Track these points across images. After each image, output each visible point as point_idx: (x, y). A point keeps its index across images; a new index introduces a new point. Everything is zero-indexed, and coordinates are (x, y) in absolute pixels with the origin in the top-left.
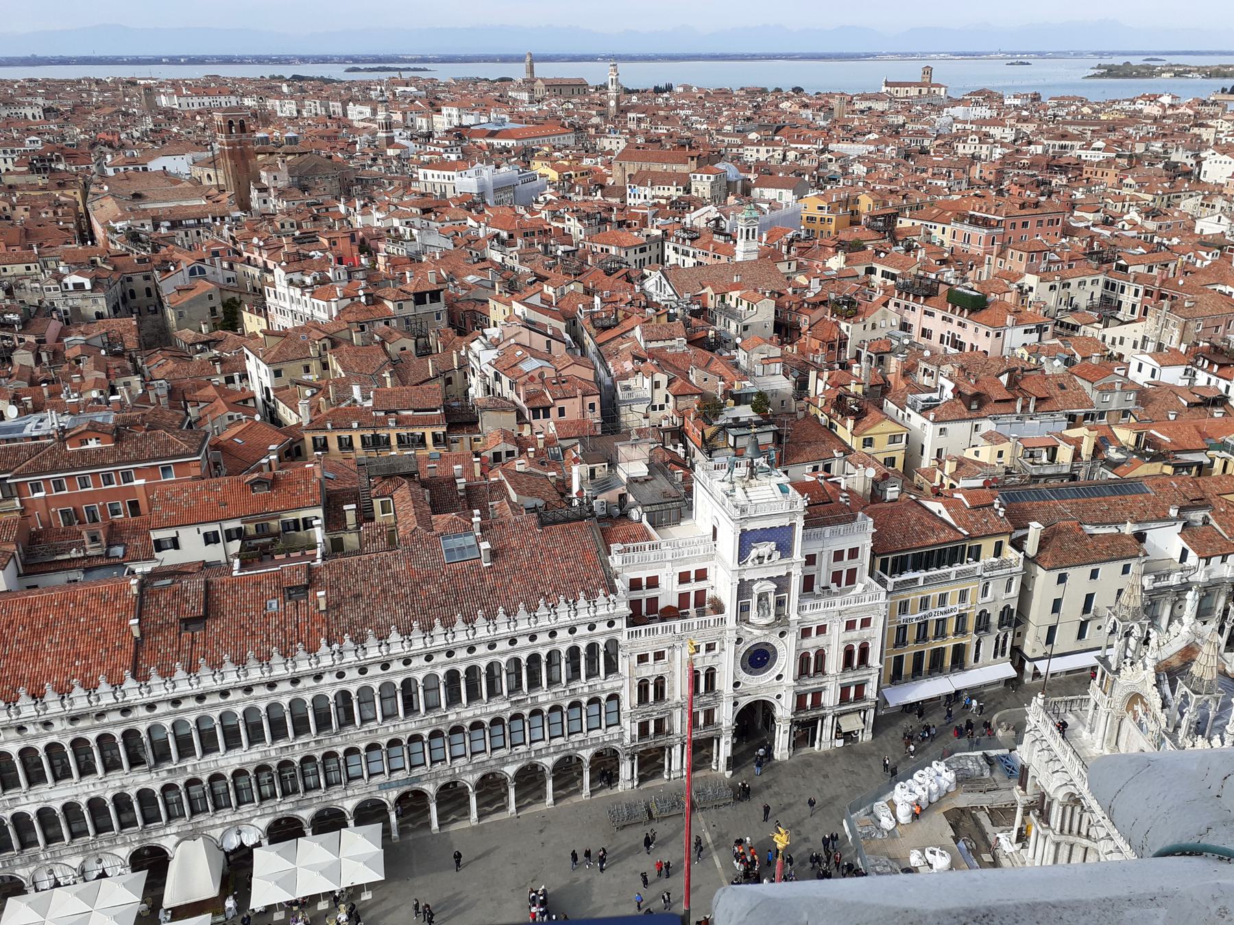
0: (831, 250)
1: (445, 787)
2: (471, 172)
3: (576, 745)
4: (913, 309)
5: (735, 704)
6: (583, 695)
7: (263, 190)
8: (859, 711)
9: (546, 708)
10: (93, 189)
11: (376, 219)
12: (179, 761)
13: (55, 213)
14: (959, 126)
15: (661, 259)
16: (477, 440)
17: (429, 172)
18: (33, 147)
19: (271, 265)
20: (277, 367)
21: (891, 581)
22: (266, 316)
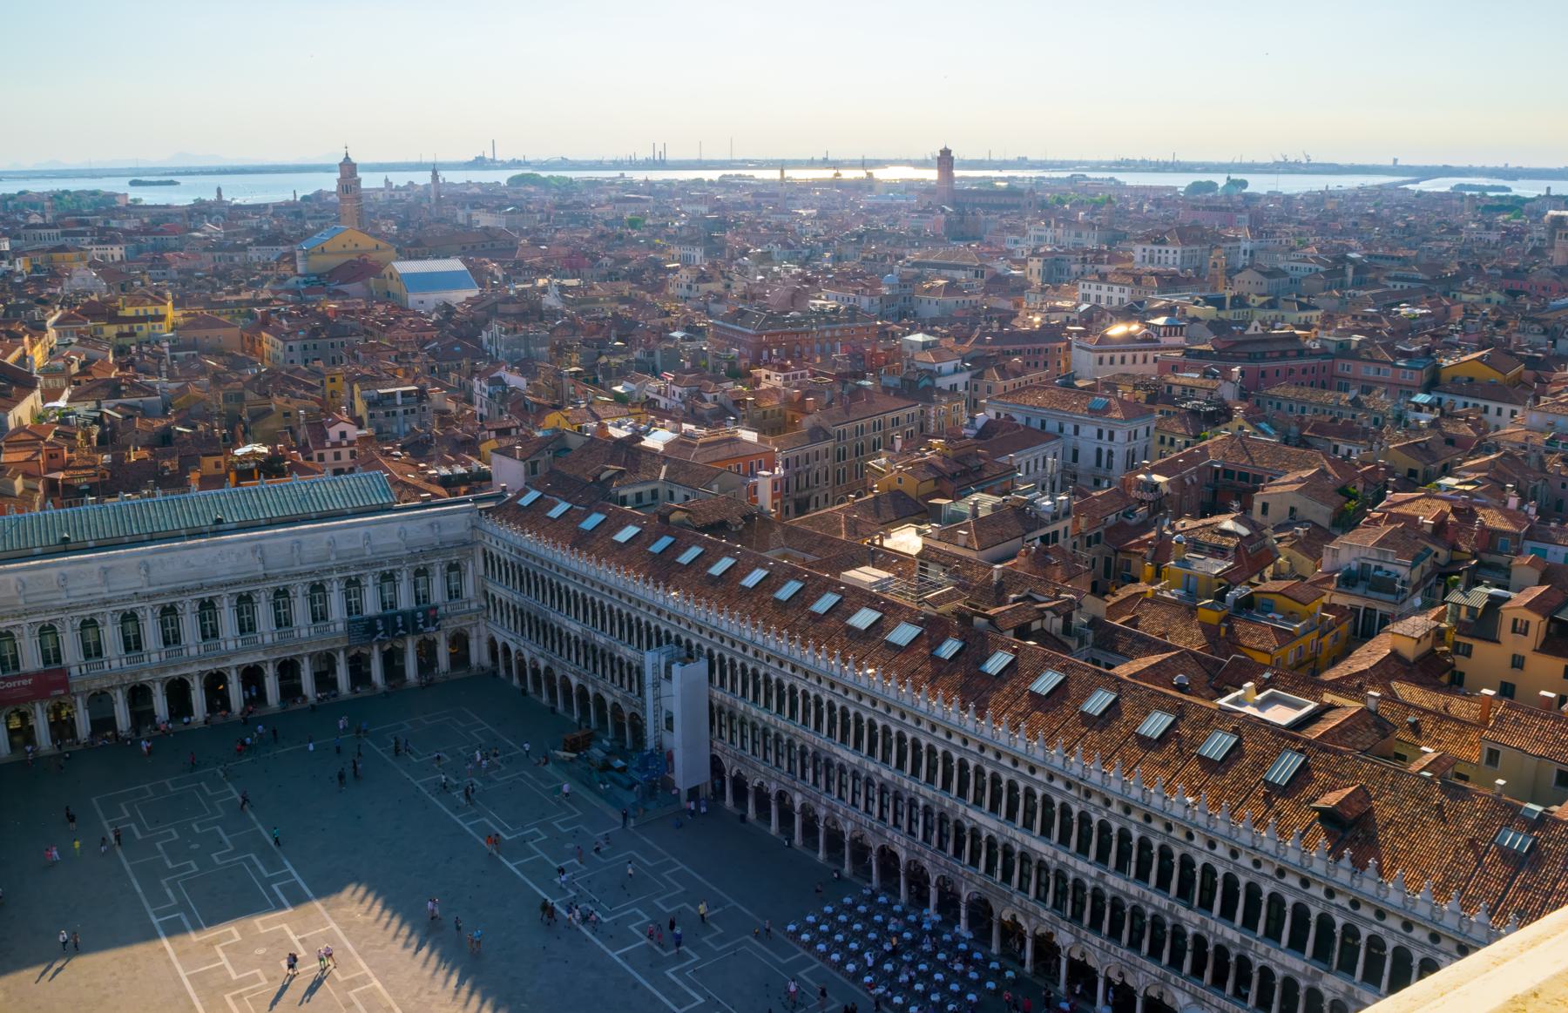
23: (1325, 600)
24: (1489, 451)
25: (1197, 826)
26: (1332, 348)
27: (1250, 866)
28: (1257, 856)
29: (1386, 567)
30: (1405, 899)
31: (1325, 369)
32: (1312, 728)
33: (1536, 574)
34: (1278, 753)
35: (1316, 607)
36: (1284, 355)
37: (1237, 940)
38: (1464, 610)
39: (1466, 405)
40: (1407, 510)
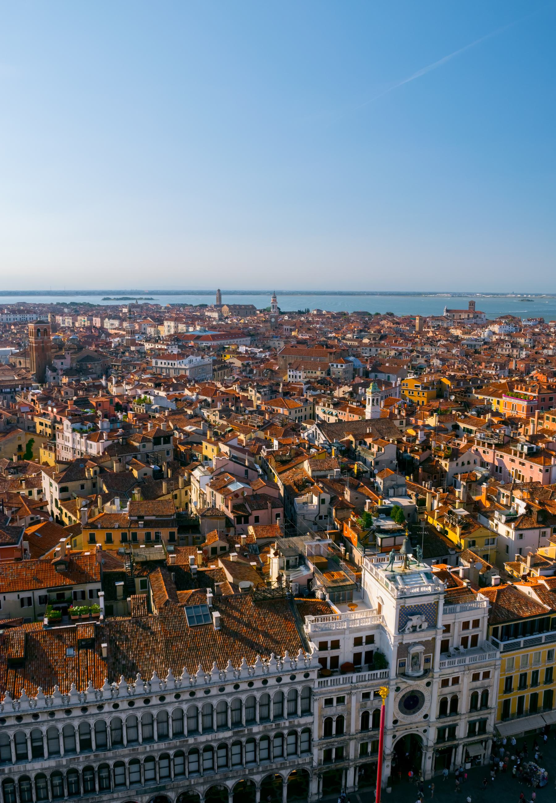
0: (428, 413)
1: (184, 794)
2: (186, 361)
3: (279, 766)
4: (488, 453)
5: (394, 737)
6: (285, 728)
7: (54, 370)
8: (481, 742)
9: (258, 737)
15: (314, 416)
16: (199, 538)
17: (159, 362)
19: (58, 419)
20: (64, 485)
21: (502, 644)
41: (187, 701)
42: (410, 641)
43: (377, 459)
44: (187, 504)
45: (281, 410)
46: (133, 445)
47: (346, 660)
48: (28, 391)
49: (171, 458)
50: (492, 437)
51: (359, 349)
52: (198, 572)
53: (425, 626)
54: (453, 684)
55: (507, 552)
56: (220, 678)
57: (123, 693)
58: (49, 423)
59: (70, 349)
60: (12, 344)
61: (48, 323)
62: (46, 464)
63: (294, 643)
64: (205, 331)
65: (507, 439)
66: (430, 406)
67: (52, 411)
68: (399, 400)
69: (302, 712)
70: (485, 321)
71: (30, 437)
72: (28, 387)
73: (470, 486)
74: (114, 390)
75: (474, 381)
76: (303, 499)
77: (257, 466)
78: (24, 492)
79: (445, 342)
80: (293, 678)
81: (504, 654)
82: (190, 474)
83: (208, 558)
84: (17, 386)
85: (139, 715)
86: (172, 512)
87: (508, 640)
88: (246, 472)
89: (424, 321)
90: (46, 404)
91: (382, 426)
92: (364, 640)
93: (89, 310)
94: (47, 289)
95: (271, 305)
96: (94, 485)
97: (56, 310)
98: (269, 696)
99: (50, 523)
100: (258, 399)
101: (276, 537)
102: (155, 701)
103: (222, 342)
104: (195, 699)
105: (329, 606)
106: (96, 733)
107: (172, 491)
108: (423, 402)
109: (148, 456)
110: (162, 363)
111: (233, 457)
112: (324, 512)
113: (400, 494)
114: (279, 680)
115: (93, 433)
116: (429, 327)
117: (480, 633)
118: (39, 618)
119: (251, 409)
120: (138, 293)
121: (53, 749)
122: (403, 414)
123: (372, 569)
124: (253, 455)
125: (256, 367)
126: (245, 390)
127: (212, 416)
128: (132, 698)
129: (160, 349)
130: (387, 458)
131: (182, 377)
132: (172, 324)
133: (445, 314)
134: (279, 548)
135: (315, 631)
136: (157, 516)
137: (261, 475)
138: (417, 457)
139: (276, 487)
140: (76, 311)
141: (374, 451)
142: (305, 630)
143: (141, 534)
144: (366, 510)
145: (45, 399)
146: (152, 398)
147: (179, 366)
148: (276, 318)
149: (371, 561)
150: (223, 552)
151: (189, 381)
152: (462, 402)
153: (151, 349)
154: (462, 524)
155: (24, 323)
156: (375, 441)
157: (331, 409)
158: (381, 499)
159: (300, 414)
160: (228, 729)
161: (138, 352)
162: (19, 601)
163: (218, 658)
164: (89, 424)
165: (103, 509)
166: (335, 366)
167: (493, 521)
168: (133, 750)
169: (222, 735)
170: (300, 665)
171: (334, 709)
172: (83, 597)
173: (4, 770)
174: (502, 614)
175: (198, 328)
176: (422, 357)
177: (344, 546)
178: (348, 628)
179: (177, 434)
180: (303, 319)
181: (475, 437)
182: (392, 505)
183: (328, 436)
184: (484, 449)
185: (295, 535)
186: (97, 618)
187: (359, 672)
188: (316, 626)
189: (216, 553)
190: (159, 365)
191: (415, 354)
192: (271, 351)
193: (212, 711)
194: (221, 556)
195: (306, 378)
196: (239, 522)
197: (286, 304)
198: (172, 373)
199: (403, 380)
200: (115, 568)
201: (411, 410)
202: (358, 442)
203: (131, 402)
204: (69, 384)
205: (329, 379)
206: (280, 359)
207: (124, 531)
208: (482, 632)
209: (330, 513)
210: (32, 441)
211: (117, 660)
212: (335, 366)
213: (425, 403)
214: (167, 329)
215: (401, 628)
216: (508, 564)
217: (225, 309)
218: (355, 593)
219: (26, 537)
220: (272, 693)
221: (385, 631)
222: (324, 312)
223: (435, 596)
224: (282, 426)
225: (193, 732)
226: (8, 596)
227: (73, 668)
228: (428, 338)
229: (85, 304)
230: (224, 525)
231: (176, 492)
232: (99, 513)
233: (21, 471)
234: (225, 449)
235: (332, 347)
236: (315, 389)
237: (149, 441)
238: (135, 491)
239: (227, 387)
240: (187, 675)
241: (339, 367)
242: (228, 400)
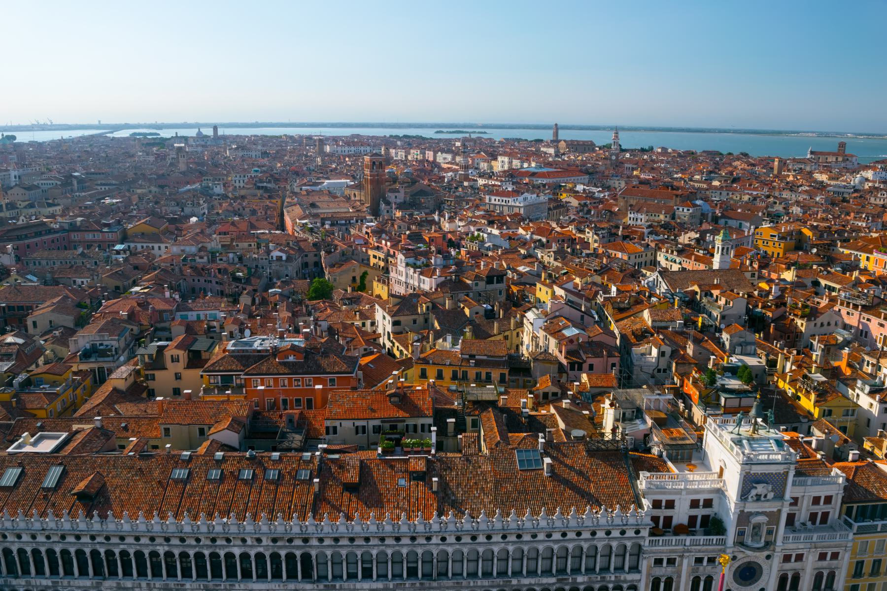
0: (784, 266)
2: (521, 198)
4: (853, 314)
6: (610, 582)
7: (388, 203)
10: (288, 200)
11: (460, 225)
12: (333, 580)
13: (266, 213)
14: (870, 184)
15: (654, 263)
16: (530, 382)
17: (493, 198)
18: (256, 174)
19: (392, 253)
20: (396, 318)
21: (856, 525)
22: (388, 285)
23: (74, 369)
24: (155, 269)
25: (7, 529)
26: (66, 227)
27: (44, 540)
28: (47, 533)
29: (105, 343)
30: (132, 526)
31: (64, 239)
32: (66, 448)
33: (183, 329)
34: (47, 469)
35: (69, 375)
36: (39, 234)
37: (50, 584)
38: (146, 357)
39: (142, 247)
40: (114, 308)
41: (513, 543)
42: (753, 510)
43: (725, 313)
44: (518, 346)
45: (619, 255)
46: (465, 283)
47: (680, 522)
48: (362, 224)
49: (503, 298)
50: (859, 297)
51: (708, 192)
52: (530, 416)
53: (771, 495)
54: (796, 561)
55: (868, 426)
56: (548, 524)
57: (451, 527)
58: (382, 256)
59: (404, 183)
60: (346, 176)
61: (381, 155)
62: (379, 296)
63: (627, 498)
64: (541, 167)
65: (876, 301)
66: (787, 258)
67: (386, 245)
68: (751, 251)
69: (630, 568)
70: (856, 166)
71: (364, 269)
72: (362, 220)
73: (829, 350)
74: (446, 226)
75: (840, 232)
76: (642, 349)
77: (594, 312)
78: (358, 323)
79: (807, 188)
80: (623, 533)
81: (857, 536)
82: (523, 316)
83: (539, 403)
84: (352, 218)
85: (465, 550)
86: (504, 353)
87: (863, 521)
88: (582, 317)
89: (783, 163)
90: (380, 237)
91: (731, 277)
92: (701, 503)
93: (421, 143)
94: (381, 121)
95: (612, 142)
96: (426, 321)
97: (390, 142)
98: (597, 548)
99: (383, 355)
100: (596, 241)
101: (612, 387)
102: (482, 539)
103: (558, 179)
104: (521, 542)
105: (665, 462)
106: (423, 562)
107: (504, 331)
108: (778, 254)
109: (480, 295)
110: (495, 200)
111: (569, 301)
112: (663, 365)
113: (748, 352)
114: (608, 533)
115: (426, 269)
116: (789, 170)
117: (831, 511)
118: (372, 447)
119: (588, 252)
120: (471, 126)
121: (381, 572)
122: (756, 266)
123: (715, 430)
124: (588, 300)
125: (594, 208)
126: (582, 231)
127: (547, 257)
128: (459, 534)
129: (494, 185)
130: (735, 312)
131: (516, 215)
132: (506, 159)
133: (809, 156)
134: (614, 399)
135: (650, 488)
136: (488, 356)
137: (597, 322)
138: (770, 314)
139: (612, 334)
140: (409, 144)
141: (719, 304)
142: (639, 486)
143: (472, 373)
144: (710, 366)
145: (379, 232)
146: (485, 235)
147: (513, 204)
148: (617, 155)
149: (715, 421)
150: (554, 398)
151: (523, 220)
152: (824, 256)
153: (485, 185)
154: (818, 390)
155: (357, 156)
156: (723, 293)
157: (675, 256)
158: (728, 357)
159: (640, 260)
160: (552, 576)
161: (472, 187)
162: (354, 429)
163: (547, 504)
164: (423, 259)
165: (435, 345)
166: (681, 209)
167: (854, 390)
168: (458, 583)
169: (545, 580)
170: (632, 521)
171: (663, 570)
172: (415, 431)
173: (335, 586)
174: (859, 493)
175: (533, 164)
176: (780, 204)
177: (683, 403)
178: (686, 489)
179: (510, 274)
180: (645, 157)
181: (839, 295)
182: (740, 364)
183: (670, 285)
184: (848, 310)
185: (629, 388)
186: (429, 452)
187: (694, 535)
188: (650, 483)
189: (547, 398)
190: (493, 202)
191: (772, 200)
192: (611, 190)
193: (538, 555)
194: (552, 402)
195: (647, 221)
196: (572, 369)
197: (628, 141)
198: (506, 211)
199: (756, 228)
200: (445, 404)
201: (765, 262)
202: (703, 293)
203: (463, 239)
204: (402, 219)
205: (673, 224)
206: (620, 200)
207: (455, 368)
208: (835, 510)
209: (670, 367)
210: (365, 273)
211: (447, 495)
212: (681, 209)
213: (781, 256)
214: (501, 164)
215: (744, 495)
216: (868, 440)
217: (562, 144)
218: (695, 454)
219: (361, 368)
220: (600, 545)
221: (725, 496)
222: (670, 150)
223: (786, 466)
224: (621, 271)
225: (517, 574)
226: (343, 422)
227: (404, 498)
228: (788, 183)
229: (418, 137)
230: (557, 370)
231: (507, 333)
232: (431, 349)
233: (355, 302)
234: (559, 292)
235: (678, 189)
236: (657, 234)
237: (482, 279)
238: (467, 330)
239: (562, 227)
240: (515, 518)
241: (685, 210)
242: (563, 241)
